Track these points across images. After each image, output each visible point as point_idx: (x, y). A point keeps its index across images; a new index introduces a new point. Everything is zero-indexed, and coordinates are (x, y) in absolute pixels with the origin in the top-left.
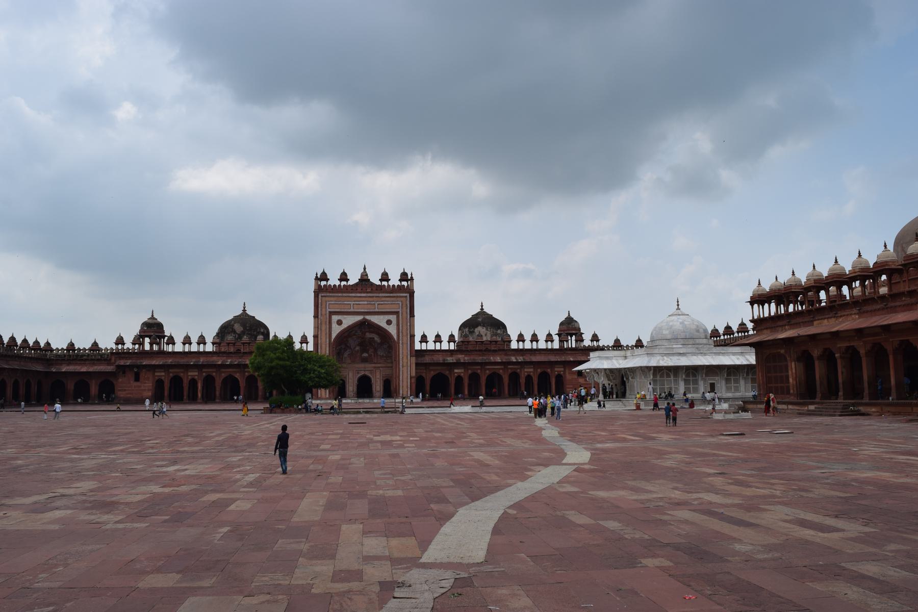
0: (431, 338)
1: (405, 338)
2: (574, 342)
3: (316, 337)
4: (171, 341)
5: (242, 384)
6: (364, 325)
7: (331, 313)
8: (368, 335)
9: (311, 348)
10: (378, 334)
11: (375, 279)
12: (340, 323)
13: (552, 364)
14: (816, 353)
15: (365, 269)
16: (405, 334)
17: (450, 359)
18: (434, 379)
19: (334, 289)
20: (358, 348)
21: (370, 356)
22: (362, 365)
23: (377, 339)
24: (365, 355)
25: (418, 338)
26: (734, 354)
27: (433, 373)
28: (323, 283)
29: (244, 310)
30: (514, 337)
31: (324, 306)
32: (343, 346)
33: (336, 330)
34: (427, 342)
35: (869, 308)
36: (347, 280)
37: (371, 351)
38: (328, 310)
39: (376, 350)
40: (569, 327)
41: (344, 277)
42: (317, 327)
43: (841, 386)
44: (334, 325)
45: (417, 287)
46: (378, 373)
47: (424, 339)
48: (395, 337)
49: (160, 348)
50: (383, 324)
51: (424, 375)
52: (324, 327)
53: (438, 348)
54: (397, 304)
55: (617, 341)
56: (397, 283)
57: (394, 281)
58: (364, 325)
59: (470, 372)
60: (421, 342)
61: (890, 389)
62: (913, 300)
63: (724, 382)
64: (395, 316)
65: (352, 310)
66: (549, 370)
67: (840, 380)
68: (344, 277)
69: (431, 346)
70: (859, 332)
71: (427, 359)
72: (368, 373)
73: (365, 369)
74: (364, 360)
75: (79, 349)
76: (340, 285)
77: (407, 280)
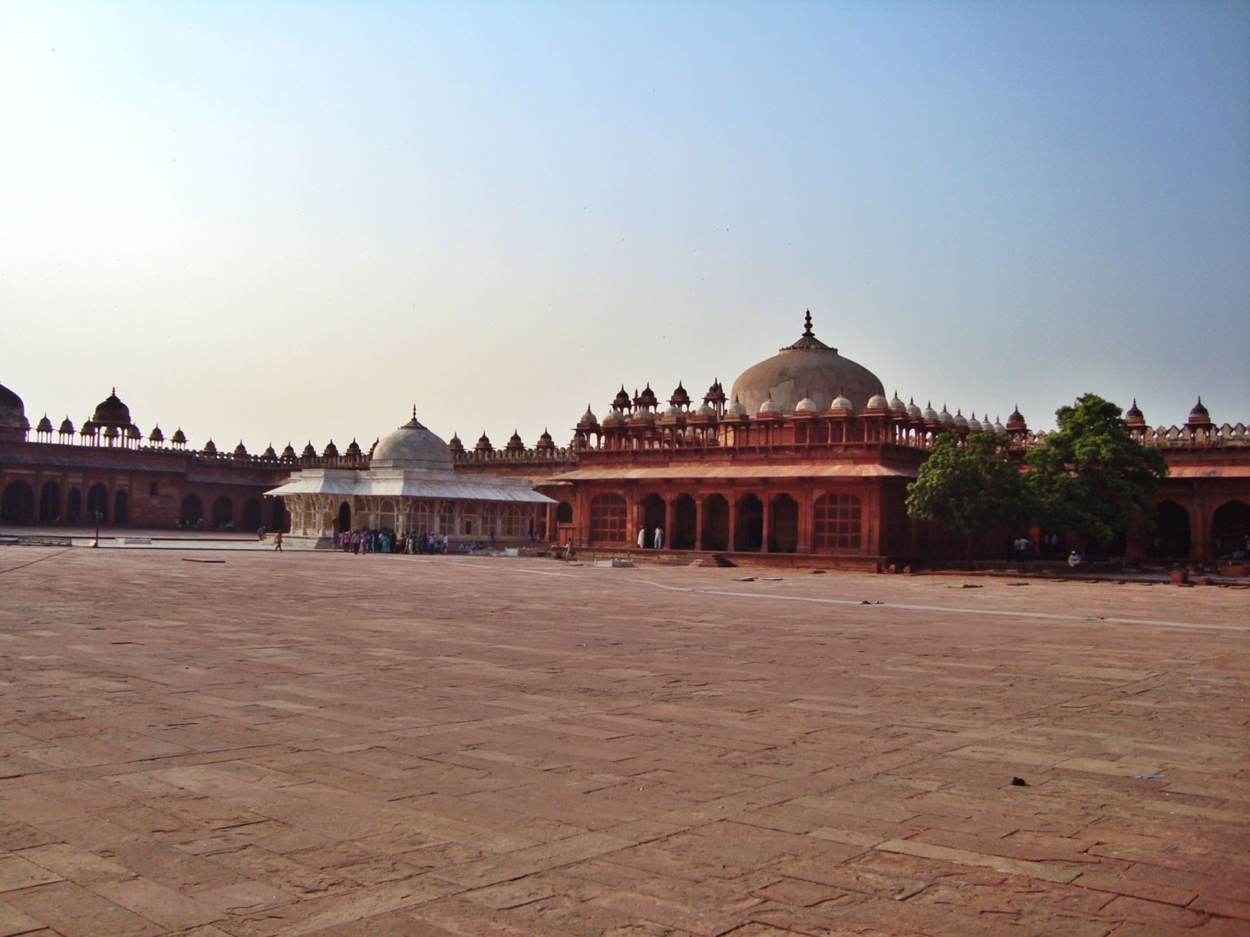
2: (102, 437)
4: (135, 433)
13: (112, 472)
14: (668, 497)
26: (495, 487)
30: (34, 422)
35: (744, 457)
40: (113, 413)
43: (699, 536)
49: (110, 444)
55: (211, 445)
61: (727, 540)
62: (798, 455)
63: (480, 522)
66: (106, 483)
67: (732, 527)
70: (732, 482)
75: (222, 454)
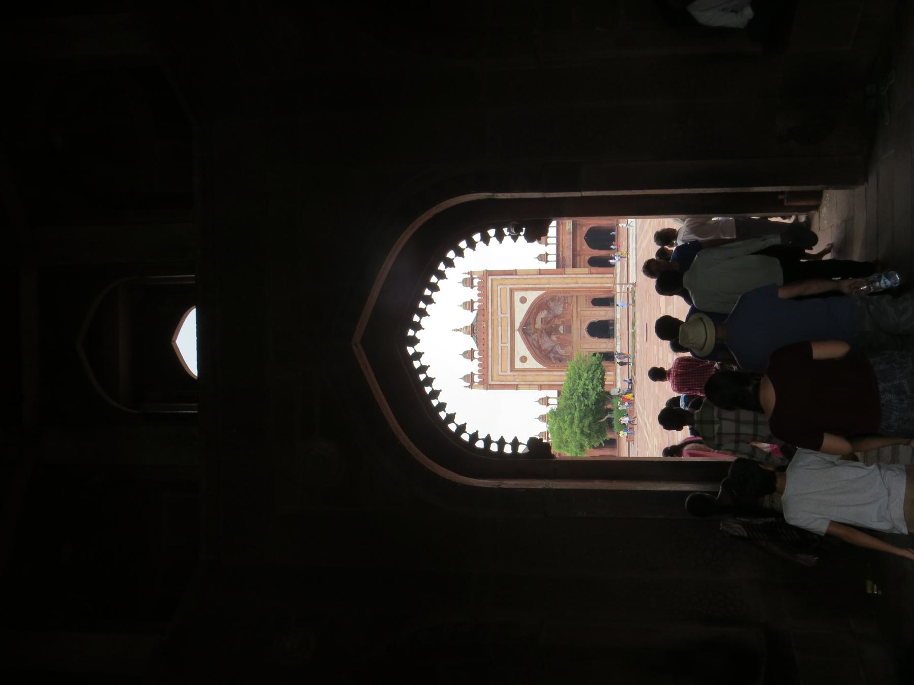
1: (543, 281)
3: (541, 387)
6: (527, 330)
7: (512, 369)
8: (538, 325)
9: (553, 393)
10: (537, 314)
11: (469, 318)
12: (524, 359)
15: (457, 330)
16: (537, 281)
19: (484, 367)
20: (554, 338)
21: (563, 323)
23: (543, 314)
24: (561, 329)
25: (543, 266)
27: (586, 246)
28: (476, 379)
31: (504, 378)
32: (552, 355)
33: (533, 363)
34: (547, 254)
36: (472, 351)
37: (557, 321)
38: (509, 373)
39: (556, 316)
41: (469, 355)
42: (530, 386)
44: (526, 365)
47: (544, 258)
48: (541, 293)
51: (587, 258)
52: (530, 377)
53: (554, 241)
54: (501, 289)
56: (475, 291)
57: (473, 294)
58: (527, 330)
60: (547, 261)
65: (508, 345)
68: (469, 355)
71: (568, 254)
74: (568, 329)
76: (479, 359)
77: (472, 279)
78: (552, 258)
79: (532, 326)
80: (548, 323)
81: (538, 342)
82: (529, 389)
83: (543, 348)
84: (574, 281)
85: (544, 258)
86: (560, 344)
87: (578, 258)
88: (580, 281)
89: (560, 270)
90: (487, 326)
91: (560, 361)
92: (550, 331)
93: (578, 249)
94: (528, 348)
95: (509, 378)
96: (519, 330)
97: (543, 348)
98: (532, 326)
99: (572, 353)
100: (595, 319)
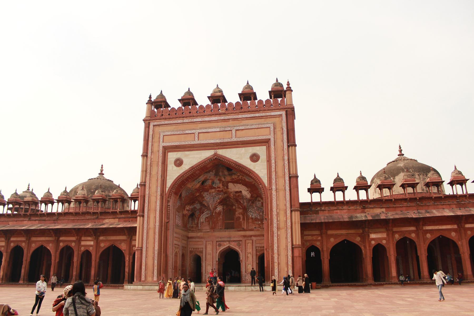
0: (327, 184)
1: (281, 181)
5: (55, 259)
8: (233, 188)
12: (179, 163)
16: (280, 173)
17: (361, 216)
18: (335, 251)
20: (219, 208)
22: (225, 234)
25: (304, 184)
27: (333, 241)
29: (101, 174)
31: (156, 139)
32: (198, 206)
33: (174, 174)
38: (162, 144)
39: (245, 210)
42: (145, 172)
44: (171, 167)
45: (297, 100)
46: (249, 246)
47: (316, 187)
50: (246, 162)
51: (318, 244)
52: (157, 170)
59: (397, 237)
64: (265, 147)
65: (197, 142)
69: (327, 196)
71: (322, 217)
72: (234, 246)
73: (230, 238)
74: (229, 227)
78: (316, 197)
79: (228, 178)
80: (237, 201)
81: (212, 187)
82: (142, 171)
83: (205, 194)
84: (282, 225)
85: (316, 187)
86: (212, 215)
87: (317, 232)
88: (282, 232)
89: (298, 206)
90: (220, 114)
91: (192, 216)
92: (228, 202)
93: (330, 232)
94: (192, 168)
95: (156, 145)
96: (215, 154)
97: (205, 194)
98: (228, 178)
99: (200, 231)
100: (242, 257)
